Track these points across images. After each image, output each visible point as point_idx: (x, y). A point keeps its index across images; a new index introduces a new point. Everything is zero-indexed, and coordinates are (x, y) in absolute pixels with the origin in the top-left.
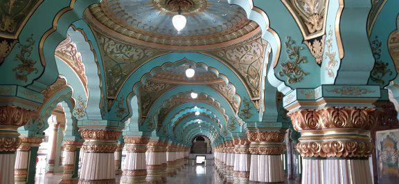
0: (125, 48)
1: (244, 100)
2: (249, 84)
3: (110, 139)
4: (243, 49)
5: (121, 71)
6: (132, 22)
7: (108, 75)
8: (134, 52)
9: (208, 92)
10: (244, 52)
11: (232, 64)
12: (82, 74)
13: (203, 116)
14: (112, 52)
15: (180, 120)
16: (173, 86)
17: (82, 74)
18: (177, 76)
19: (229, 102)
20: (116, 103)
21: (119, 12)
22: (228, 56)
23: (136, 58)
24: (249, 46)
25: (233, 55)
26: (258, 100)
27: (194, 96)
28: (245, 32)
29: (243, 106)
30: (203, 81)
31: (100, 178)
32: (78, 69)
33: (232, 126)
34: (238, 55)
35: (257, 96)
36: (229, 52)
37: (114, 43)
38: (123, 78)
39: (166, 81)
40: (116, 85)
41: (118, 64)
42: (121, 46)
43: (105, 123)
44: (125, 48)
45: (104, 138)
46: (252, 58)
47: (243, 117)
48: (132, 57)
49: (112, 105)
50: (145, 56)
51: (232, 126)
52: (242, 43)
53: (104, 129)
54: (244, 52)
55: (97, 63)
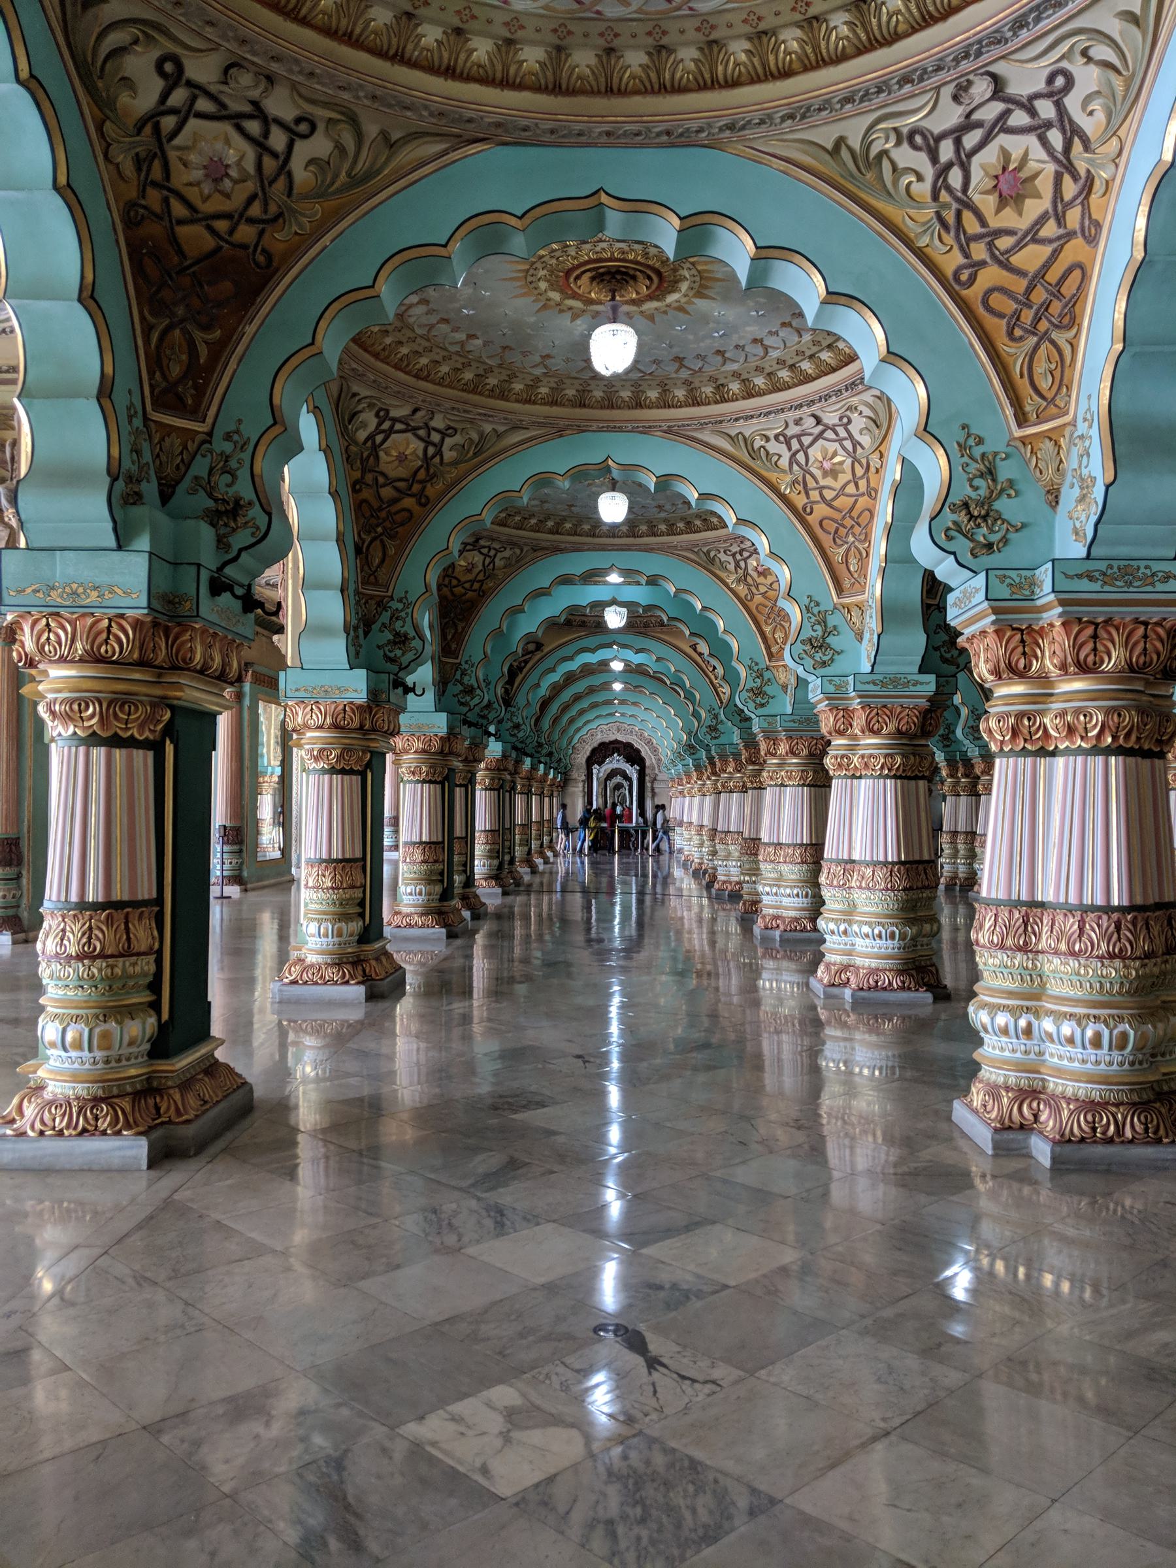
12: (974, 293)
17: (974, 293)
32: (952, 261)
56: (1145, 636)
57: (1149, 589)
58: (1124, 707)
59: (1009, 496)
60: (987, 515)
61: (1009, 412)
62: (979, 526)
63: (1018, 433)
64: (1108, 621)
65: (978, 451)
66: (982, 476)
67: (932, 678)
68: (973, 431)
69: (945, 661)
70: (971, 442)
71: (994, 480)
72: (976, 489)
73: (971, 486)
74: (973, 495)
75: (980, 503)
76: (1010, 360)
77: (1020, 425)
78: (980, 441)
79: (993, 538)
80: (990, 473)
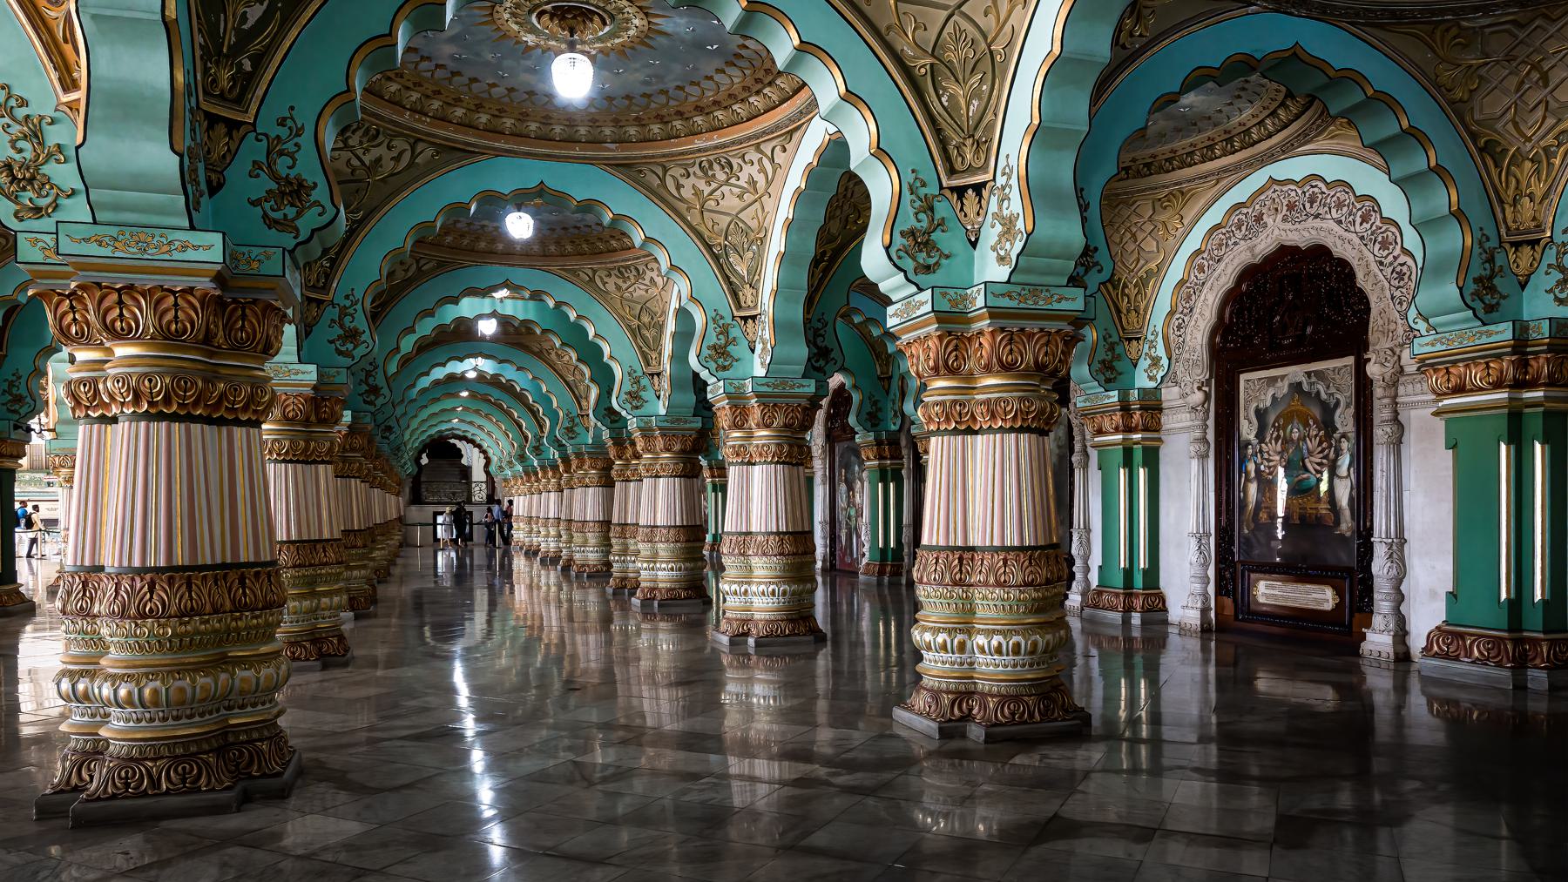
1: (912, 187)
3: (237, 348)
9: (620, 200)
13: (515, 336)
16: (466, 154)
18: (479, 107)
19: (709, 247)
26: (978, 188)
27: (520, 226)
29: (908, 210)
30: (596, 142)
35: (971, 170)
47: (909, 264)
53: (204, 284)
56: (176, 304)
57: (166, 257)
58: (158, 373)
59: (58, 161)
60: (33, 178)
61: (54, 76)
62: (24, 189)
63: (65, 98)
64: (130, 288)
65: (20, 113)
66: (25, 137)
67: (312, 368)
68: (16, 91)
69: (340, 353)
70: (12, 102)
71: (41, 144)
72: (20, 151)
73: (14, 147)
74: (17, 157)
75: (24, 166)
76: (53, 24)
77: (66, 90)
78: (23, 103)
79: (43, 202)
80: (36, 135)
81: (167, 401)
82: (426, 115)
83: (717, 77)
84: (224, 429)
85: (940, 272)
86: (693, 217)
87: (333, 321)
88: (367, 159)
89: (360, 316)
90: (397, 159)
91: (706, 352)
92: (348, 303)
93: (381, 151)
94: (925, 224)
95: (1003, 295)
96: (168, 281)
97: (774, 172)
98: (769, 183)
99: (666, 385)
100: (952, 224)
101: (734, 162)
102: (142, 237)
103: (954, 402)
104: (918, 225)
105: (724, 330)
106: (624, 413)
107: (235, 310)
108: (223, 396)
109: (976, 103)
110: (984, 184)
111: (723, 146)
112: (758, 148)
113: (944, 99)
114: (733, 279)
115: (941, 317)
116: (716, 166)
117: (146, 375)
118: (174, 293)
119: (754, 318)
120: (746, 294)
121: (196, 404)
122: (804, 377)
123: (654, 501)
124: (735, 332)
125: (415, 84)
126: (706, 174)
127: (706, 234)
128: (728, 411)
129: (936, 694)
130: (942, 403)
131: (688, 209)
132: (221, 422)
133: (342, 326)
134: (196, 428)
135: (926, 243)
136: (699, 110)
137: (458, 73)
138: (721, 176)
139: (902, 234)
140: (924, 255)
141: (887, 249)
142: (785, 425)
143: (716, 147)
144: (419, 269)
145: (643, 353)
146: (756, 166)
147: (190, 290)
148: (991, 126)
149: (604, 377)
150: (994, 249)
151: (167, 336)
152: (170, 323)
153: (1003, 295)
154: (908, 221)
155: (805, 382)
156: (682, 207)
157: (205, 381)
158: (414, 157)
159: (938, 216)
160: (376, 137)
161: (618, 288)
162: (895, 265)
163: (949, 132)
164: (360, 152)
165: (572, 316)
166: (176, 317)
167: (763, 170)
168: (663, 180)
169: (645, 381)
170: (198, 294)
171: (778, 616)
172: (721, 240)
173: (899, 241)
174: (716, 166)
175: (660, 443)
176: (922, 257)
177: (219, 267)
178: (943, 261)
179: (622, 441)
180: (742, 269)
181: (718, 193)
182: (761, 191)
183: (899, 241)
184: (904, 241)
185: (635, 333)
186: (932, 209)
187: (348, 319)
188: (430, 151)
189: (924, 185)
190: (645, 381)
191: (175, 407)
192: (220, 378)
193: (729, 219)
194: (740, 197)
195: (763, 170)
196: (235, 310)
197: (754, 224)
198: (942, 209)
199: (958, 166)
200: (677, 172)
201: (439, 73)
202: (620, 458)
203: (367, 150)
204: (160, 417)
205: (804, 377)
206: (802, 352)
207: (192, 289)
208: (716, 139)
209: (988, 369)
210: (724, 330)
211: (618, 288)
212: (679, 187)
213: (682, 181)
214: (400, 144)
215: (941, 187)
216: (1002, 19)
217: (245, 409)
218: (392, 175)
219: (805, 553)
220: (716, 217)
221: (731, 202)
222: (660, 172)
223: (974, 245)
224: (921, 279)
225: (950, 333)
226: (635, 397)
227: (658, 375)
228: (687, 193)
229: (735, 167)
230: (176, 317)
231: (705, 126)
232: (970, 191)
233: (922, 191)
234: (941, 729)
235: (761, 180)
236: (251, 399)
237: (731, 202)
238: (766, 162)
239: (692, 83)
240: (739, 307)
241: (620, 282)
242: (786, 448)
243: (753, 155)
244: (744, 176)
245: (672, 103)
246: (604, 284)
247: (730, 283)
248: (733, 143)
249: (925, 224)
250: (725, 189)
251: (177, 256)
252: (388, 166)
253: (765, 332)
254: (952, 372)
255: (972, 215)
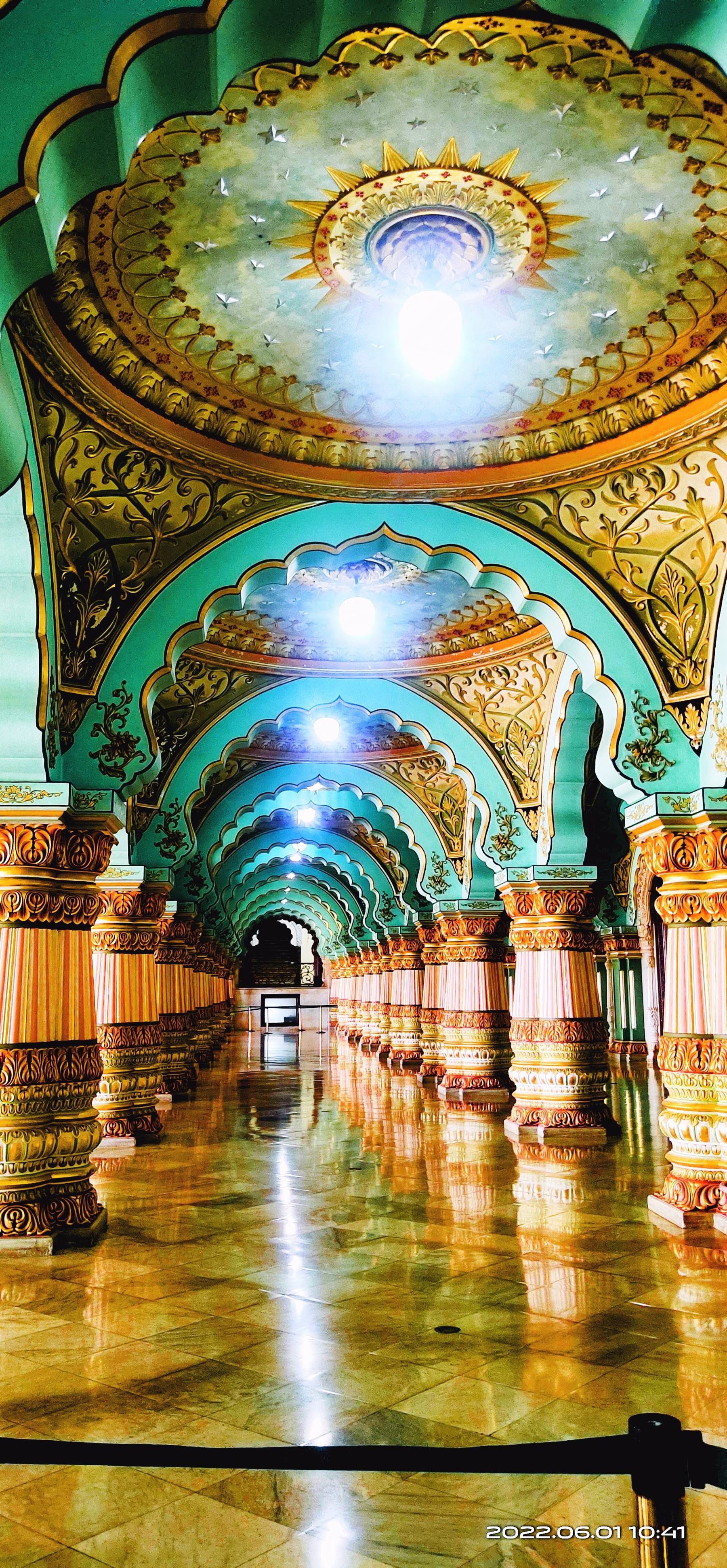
0: (140, 468)
2: (655, 635)
3: (76, 868)
4: (638, 482)
5: (116, 574)
6: (193, 338)
7: (64, 583)
8: (171, 494)
10: (645, 498)
11: (582, 550)
14: (84, 483)
15: (246, 836)
19: (491, 746)
20: (95, 715)
21: (151, 277)
22: (564, 513)
23: (178, 519)
24: (667, 470)
25: (592, 514)
26: (697, 703)
28: (675, 399)
31: (42, 1038)
33: (504, 841)
34: (612, 513)
35: (690, 687)
36: (576, 498)
37: (95, 444)
38: (124, 609)
39: (237, 659)
40: (92, 634)
41: (105, 544)
42: (121, 460)
43: (59, 796)
44: (140, 468)
45: (53, 865)
46: (676, 524)
48: (162, 513)
49: (79, 720)
50: (216, 511)
51: (504, 841)
52: (644, 453)
53: (54, 822)
54: (645, 498)
55: (29, 520)
56: (34, 838)
57: (29, 803)
69: (164, 854)
81: (23, 912)
82: (241, 650)
83: (487, 601)
84: (63, 932)
85: (664, 778)
86: (476, 720)
87: (160, 827)
88: (191, 689)
89: (182, 821)
90: (216, 687)
91: (489, 843)
92: (172, 811)
93: (204, 681)
94: (650, 737)
95: (721, 799)
96: (30, 821)
97: (548, 676)
98: (543, 686)
99: (467, 870)
100: (676, 734)
101: (511, 669)
102: (14, 789)
103: (685, 897)
104: (643, 738)
105: (508, 822)
106: (428, 898)
107: (75, 839)
108: (63, 907)
109: (690, 629)
110: (702, 700)
111: (499, 657)
112: (531, 655)
113: (662, 628)
114: (514, 773)
115: (667, 820)
116: (494, 674)
117: (9, 892)
118: (32, 829)
119: (535, 809)
120: (527, 787)
121: (43, 914)
122: (586, 863)
123: (461, 983)
124: (516, 823)
125: (230, 627)
126: (486, 681)
127: (488, 734)
128: (513, 900)
129: (683, 1183)
130: (675, 897)
131: (471, 713)
132: (61, 927)
133: (166, 830)
134: (42, 932)
135: (651, 755)
136: (475, 628)
137: (267, 615)
138: (499, 682)
139: (628, 747)
140: (649, 764)
141: (614, 760)
142: (568, 912)
143: (493, 658)
144: (241, 769)
145: (445, 838)
146: (531, 672)
147: (44, 827)
148: (703, 650)
149: (411, 862)
150: (714, 757)
151: (26, 862)
152: (28, 852)
153: (721, 799)
154: (633, 734)
155: (588, 869)
156: (465, 711)
157: (51, 895)
158: (230, 683)
159: (661, 729)
160: (198, 671)
161: (421, 777)
162: (622, 774)
163: (669, 656)
164: (186, 684)
165: (379, 806)
166: (33, 847)
167: (537, 675)
168: (447, 688)
169: (448, 866)
170: (49, 829)
171: (563, 1105)
172: (503, 739)
173: (624, 754)
174: (494, 674)
175: (463, 926)
176: (647, 766)
177: (65, 809)
178: (668, 768)
179: (429, 924)
180: (522, 764)
181: (498, 696)
182: (536, 693)
183: (624, 754)
184: (630, 753)
185: (437, 819)
186: (655, 723)
187: (172, 824)
188: (243, 678)
189: (647, 702)
190: (448, 866)
191: (28, 916)
192: (62, 893)
193: (509, 719)
194: (518, 699)
195: (537, 675)
196: (75, 839)
197: (532, 723)
198: (665, 722)
199: (679, 684)
200: (460, 680)
201: (250, 617)
202: (429, 941)
203: (192, 682)
204: (18, 924)
205: (586, 863)
206: (580, 841)
207: (45, 826)
208: (492, 652)
209: (714, 865)
210: (508, 822)
211: (421, 777)
212: (461, 693)
213: (465, 688)
214: (219, 674)
215: (664, 704)
216: (707, 558)
217: (79, 916)
218: (212, 700)
219: (595, 1041)
220: (498, 718)
221: (510, 705)
222: (444, 680)
223: (698, 752)
224: (648, 786)
225: (676, 834)
226: (438, 881)
227: (461, 859)
228: (469, 698)
229: (512, 673)
230: (33, 847)
231: (481, 641)
232: (690, 706)
233: (645, 709)
234: (686, 1218)
235: (536, 684)
236: (84, 908)
237: (510, 705)
238: (540, 668)
239: (467, 607)
240: (521, 799)
241: (422, 772)
242: (569, 933)
243: (526, 662)
244: (520, 681)
245: (450, 624)
246: (408, 775)
247: (512, 778)
248: (508, 654)
249: (650, 737)
250: (504, 693)
251: (36, 802)
252: (209, 692)
253: (543, 822)
254: (682, 868)
255: (694, 726)
